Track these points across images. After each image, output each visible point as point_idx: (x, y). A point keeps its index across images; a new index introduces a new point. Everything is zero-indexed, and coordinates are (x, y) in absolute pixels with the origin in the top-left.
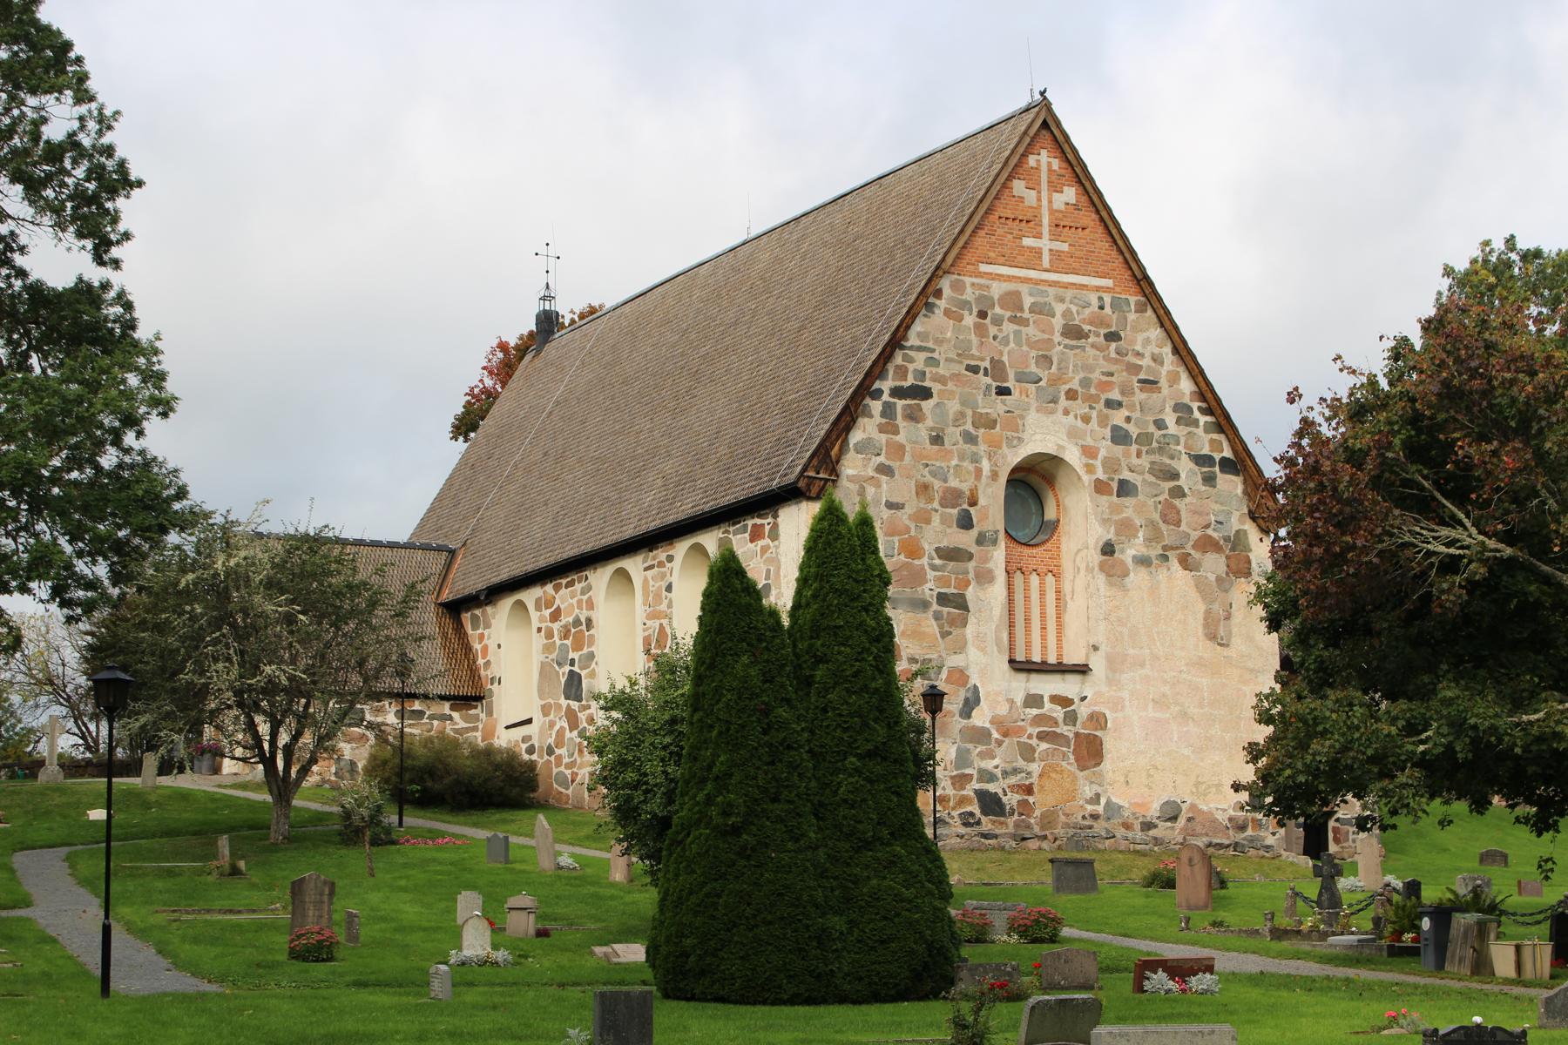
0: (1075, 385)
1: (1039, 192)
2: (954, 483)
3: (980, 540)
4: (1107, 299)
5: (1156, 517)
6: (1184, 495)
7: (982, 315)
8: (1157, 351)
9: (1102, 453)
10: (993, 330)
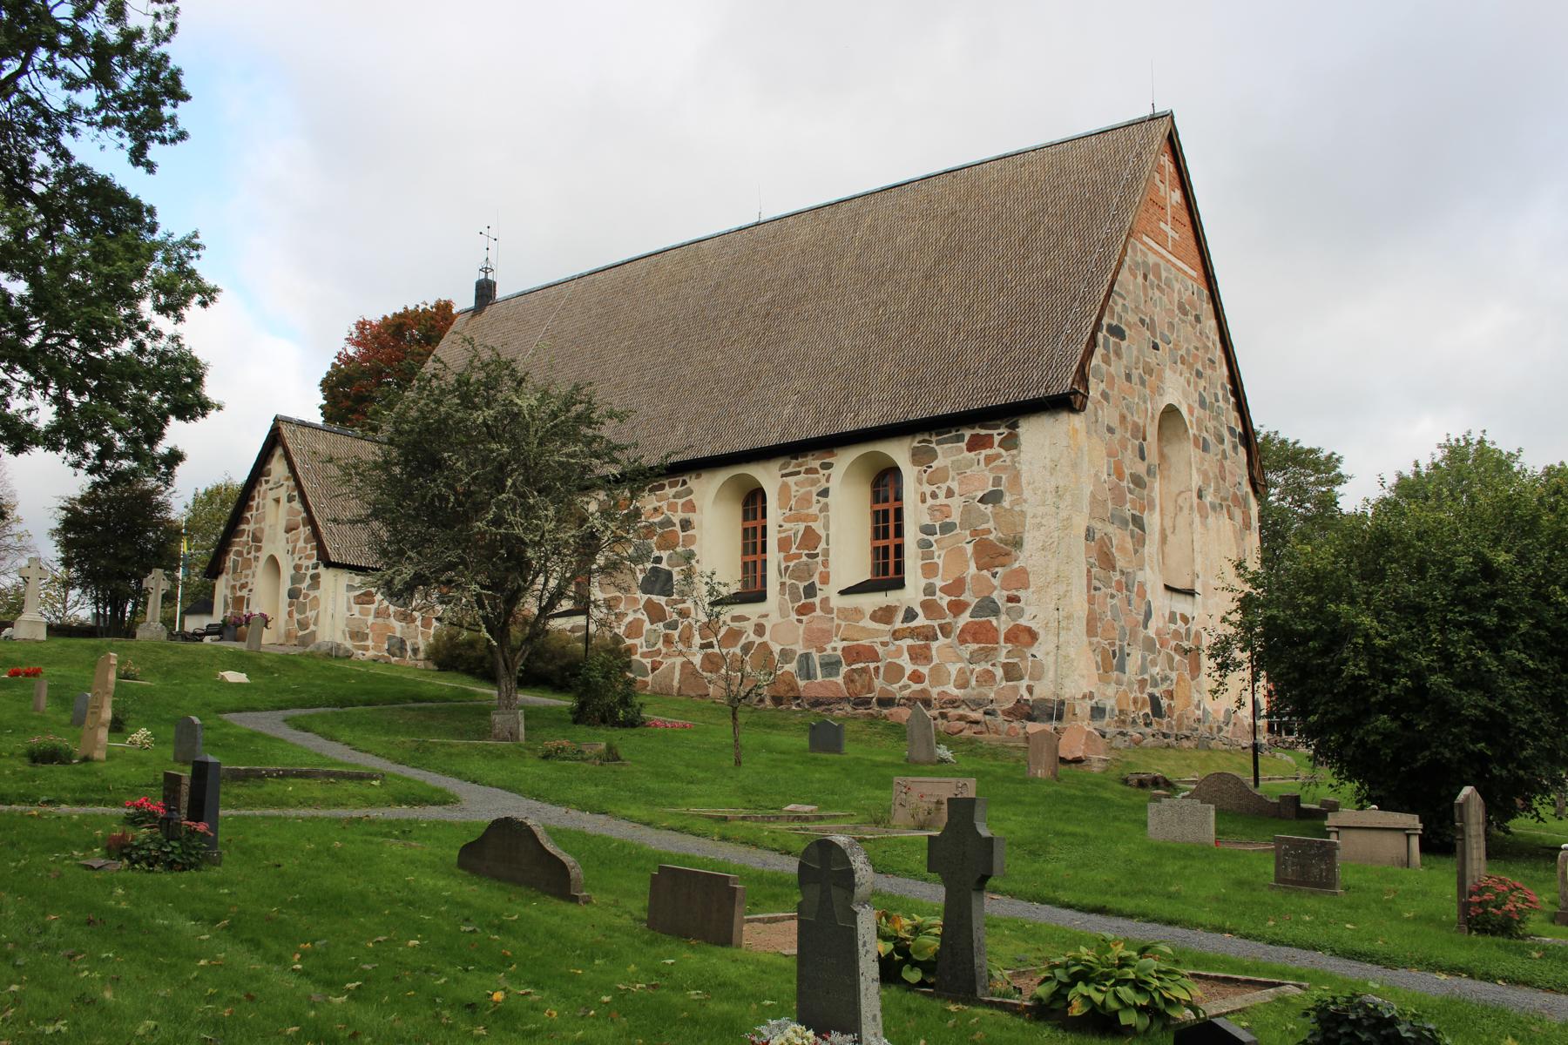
0: (1182, 352)
2: (1136, 419)
3: (1149, 472)
5: (1217, 471)
7: (1145, 277)
9: (1196, 414)
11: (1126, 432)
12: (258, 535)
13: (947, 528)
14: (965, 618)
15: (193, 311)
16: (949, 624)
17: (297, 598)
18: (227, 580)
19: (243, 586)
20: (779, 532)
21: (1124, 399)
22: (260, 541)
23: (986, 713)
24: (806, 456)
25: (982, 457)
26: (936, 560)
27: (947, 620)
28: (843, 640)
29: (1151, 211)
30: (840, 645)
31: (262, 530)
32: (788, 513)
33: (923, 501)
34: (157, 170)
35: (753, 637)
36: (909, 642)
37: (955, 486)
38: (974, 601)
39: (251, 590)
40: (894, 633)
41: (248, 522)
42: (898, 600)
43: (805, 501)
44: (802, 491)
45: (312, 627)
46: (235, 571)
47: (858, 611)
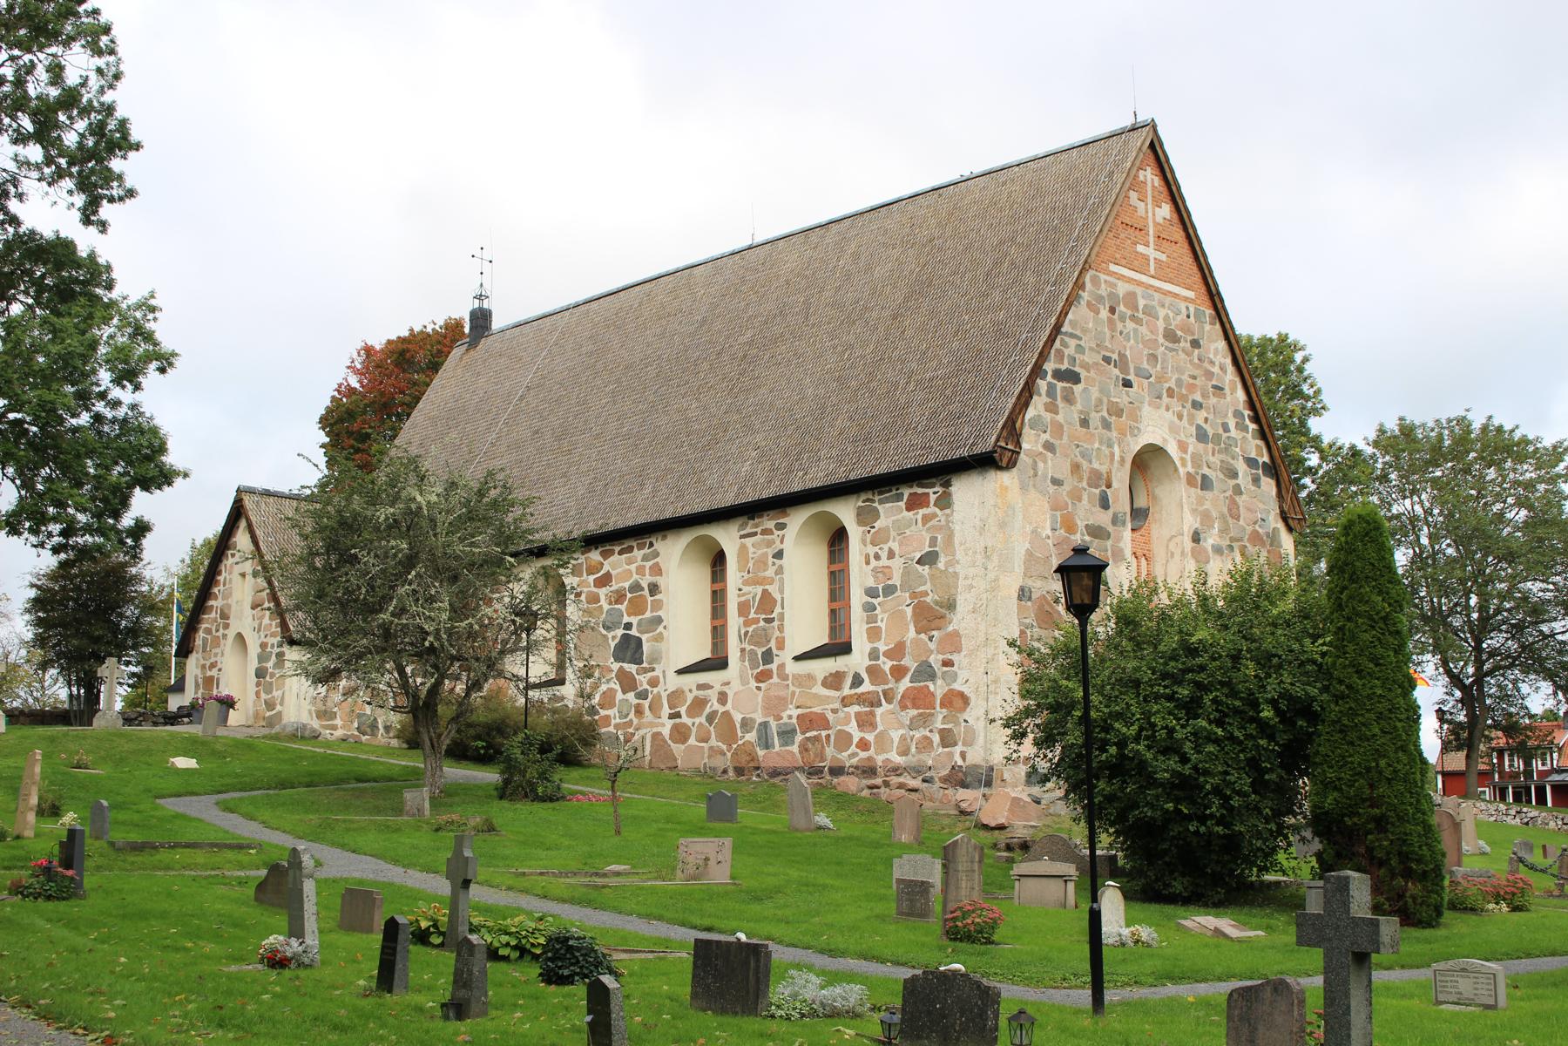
0: (1172, 384)
1: (1146, 205)
2: (1096, 465)
3: (1115, 521)
4: (1192, 310)
5: (1225, 510)
6: (1241, 493)
7: (1112, 310)
8: (1223, 360)
9: (1191, 449)
10: (1120, 326)
11: (1081, 479)
12: (226, 611)
13: (889, 590)
14: (906, 683)
15: (150, 378)
16: (891, 689)
17: (264, 678)
18: (198, 659)
19: (213, 665)
20: (739, 596)
21: (1078, 446)
22: (228, 618)
23: (924, 781)
24: (761, 516)
25: (919, 517)
26: (879, 624)
27: (890, 686)
28: (798, 707)
29: (1122, 236)
30: (795, 713)
31: (229, 606)
32: (746, 576)
33: (868, 563)
34: (110, 230)
35: (716, 706)
36: (856, 708)
37: (895, 546)
38: (913, 666)
39: (220, 670)
40: (843, 699)
41: (216, 598)
42: (846, 666)
43: (761, 563)
44: (760, 552)
45: (278, 708)
46: (204, 651)
47: (810, 677)
